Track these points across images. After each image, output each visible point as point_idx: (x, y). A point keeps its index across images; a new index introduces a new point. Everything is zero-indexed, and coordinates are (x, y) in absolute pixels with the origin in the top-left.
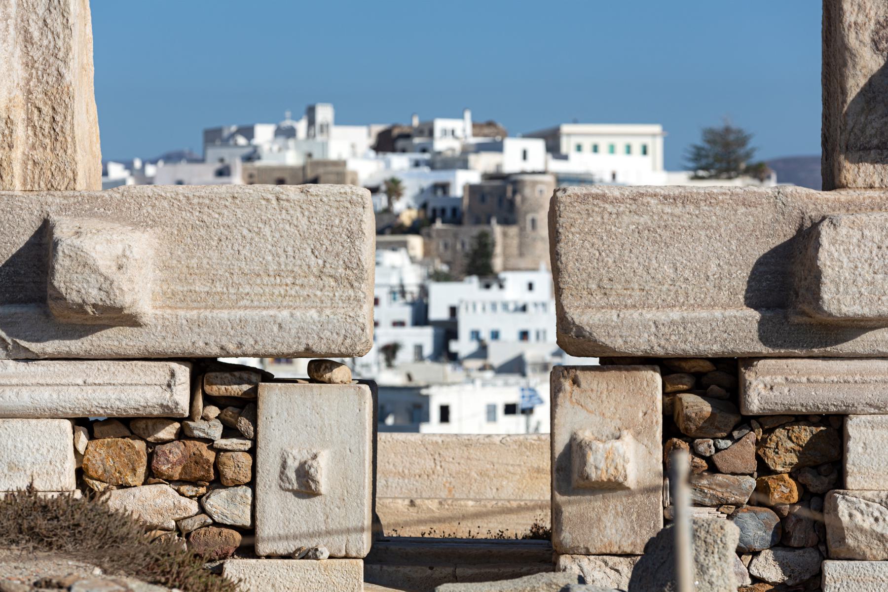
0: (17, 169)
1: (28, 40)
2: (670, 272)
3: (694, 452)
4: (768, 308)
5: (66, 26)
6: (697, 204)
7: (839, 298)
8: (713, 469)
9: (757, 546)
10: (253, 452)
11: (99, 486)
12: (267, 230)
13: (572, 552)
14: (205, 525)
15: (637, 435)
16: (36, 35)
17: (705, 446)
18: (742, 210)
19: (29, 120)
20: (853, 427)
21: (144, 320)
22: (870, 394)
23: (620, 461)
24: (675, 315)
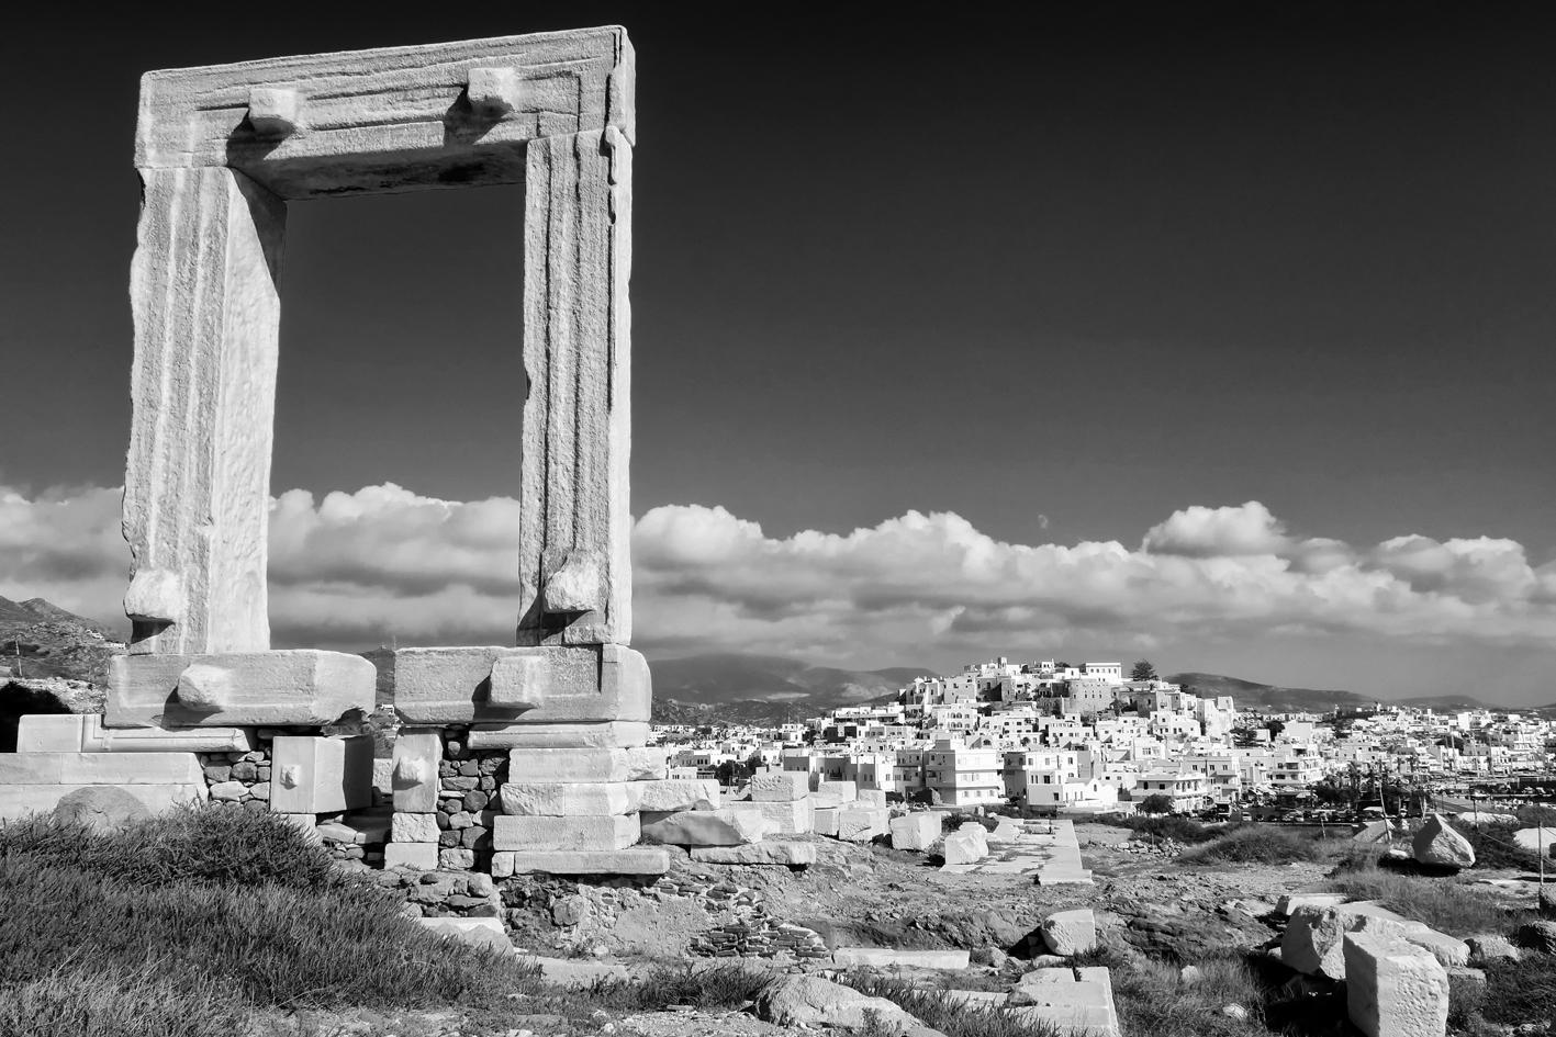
0: (182, 644)
1: (191, 590)
2: (439, 684)
3: (452, 766)
4: (479, 700)
5: (207, 584)
6: (452, 654)
7: (499, 696)
8: (459, 774)
9: (475, 809)
10: (270, 766)
11: (210, 781)
12: (277, 670)
13: (399, 811)
14: (250, 799)
15: (426, 759)
16: (194, 587)
17: (457, 764)
18: (471, 657)
19: (190, 624)
20: (511, 754)
21: (222, 709)
22: (520, 739)
23: (413, 770)
24: (439, 704)
